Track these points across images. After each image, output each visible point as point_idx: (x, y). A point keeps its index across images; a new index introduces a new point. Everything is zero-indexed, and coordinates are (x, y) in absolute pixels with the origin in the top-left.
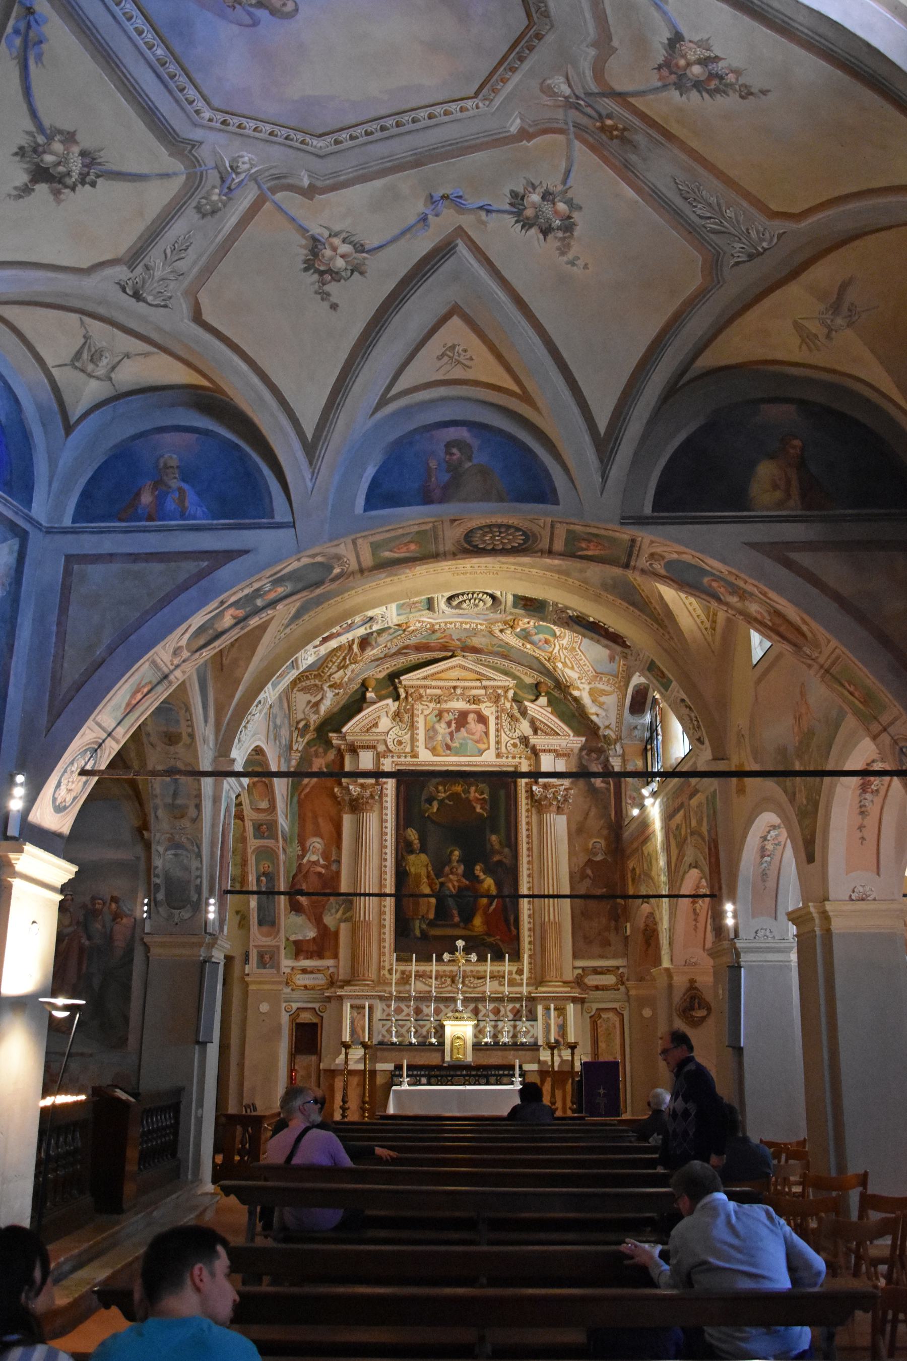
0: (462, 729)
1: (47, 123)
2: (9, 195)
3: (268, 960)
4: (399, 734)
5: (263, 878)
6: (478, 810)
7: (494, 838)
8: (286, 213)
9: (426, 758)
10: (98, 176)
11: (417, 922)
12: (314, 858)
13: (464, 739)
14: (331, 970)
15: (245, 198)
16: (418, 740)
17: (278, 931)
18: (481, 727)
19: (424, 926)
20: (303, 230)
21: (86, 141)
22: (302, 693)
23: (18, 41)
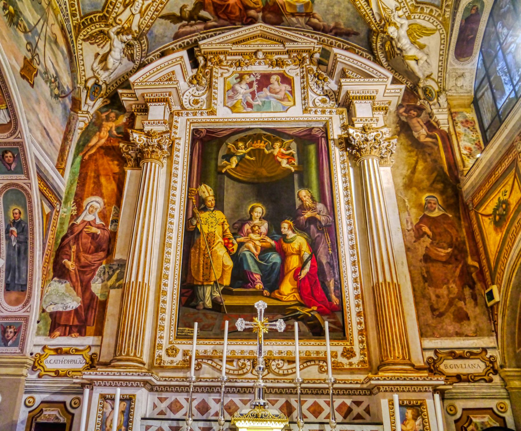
0: (265, 89)
3: (12, 334)
4: (197, 94)
5: (13, 229)
6: (284, 164)
7: (304, 193)
9: (224, 115)
11: (209, 289)
12: (90, 218)
13: (267, 98)
14: (93, 350)
16: (216, 99)
17: (29, 297)
18: (285, 87)
19: (217, 295)
22: (88, 43)
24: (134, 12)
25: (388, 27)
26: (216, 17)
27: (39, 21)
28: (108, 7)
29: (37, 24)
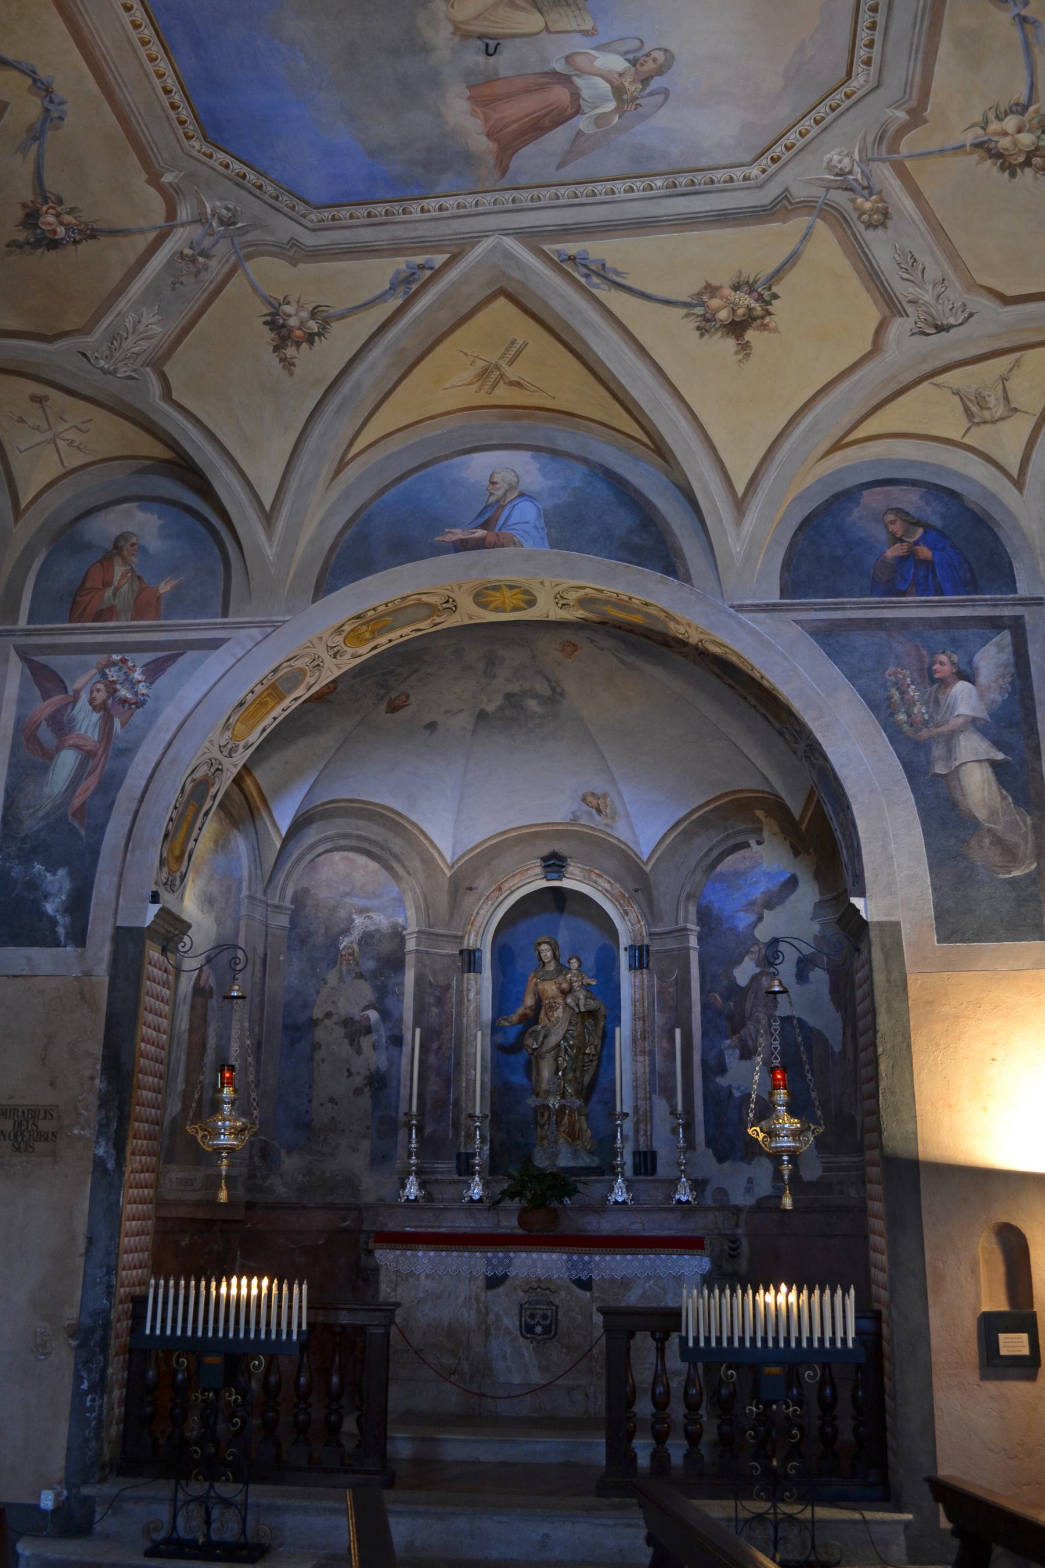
1: (685, 299)
2: (740, 361)
8: (930, 153)
10: (769, 289)
15: (887, 179)
20: (959, 149)
21: (723, 279)
23: (596, 280)
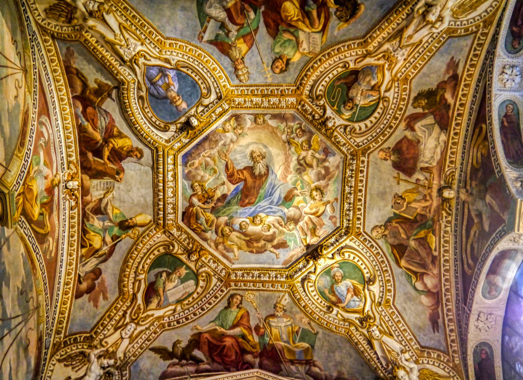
22: (62, 364)
24: (124, 335)
25: (397, 370)
26: (210, 359)
27: (18, 316)
28: (98, 328)
29: (14, 318)
